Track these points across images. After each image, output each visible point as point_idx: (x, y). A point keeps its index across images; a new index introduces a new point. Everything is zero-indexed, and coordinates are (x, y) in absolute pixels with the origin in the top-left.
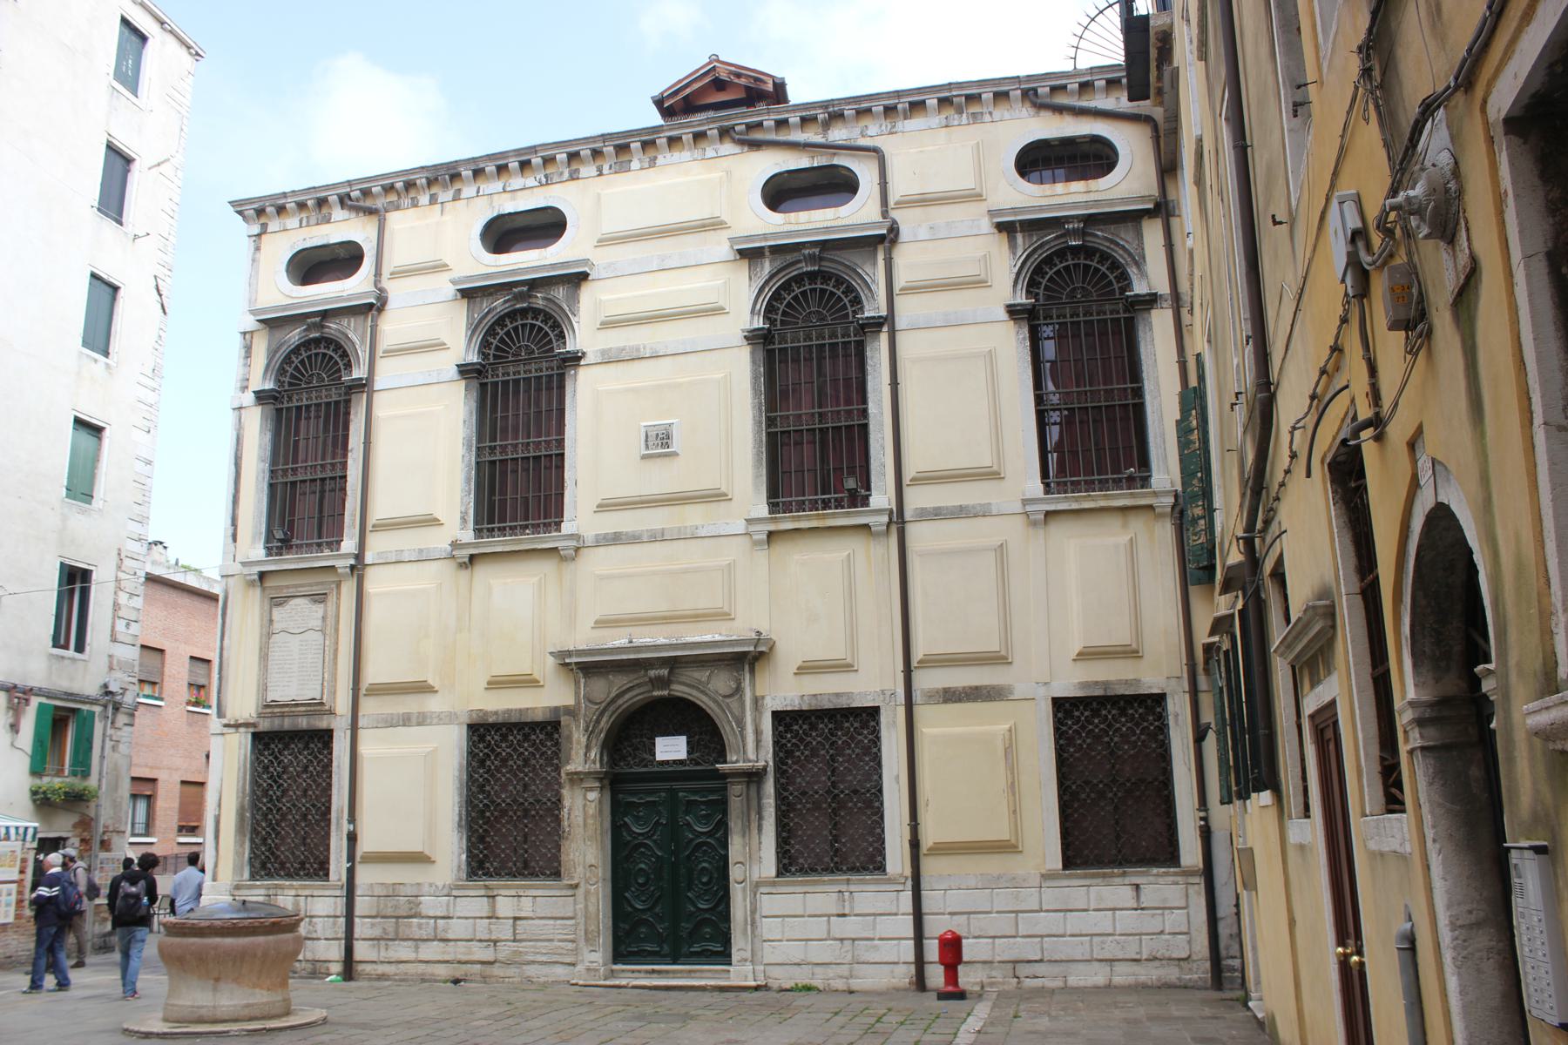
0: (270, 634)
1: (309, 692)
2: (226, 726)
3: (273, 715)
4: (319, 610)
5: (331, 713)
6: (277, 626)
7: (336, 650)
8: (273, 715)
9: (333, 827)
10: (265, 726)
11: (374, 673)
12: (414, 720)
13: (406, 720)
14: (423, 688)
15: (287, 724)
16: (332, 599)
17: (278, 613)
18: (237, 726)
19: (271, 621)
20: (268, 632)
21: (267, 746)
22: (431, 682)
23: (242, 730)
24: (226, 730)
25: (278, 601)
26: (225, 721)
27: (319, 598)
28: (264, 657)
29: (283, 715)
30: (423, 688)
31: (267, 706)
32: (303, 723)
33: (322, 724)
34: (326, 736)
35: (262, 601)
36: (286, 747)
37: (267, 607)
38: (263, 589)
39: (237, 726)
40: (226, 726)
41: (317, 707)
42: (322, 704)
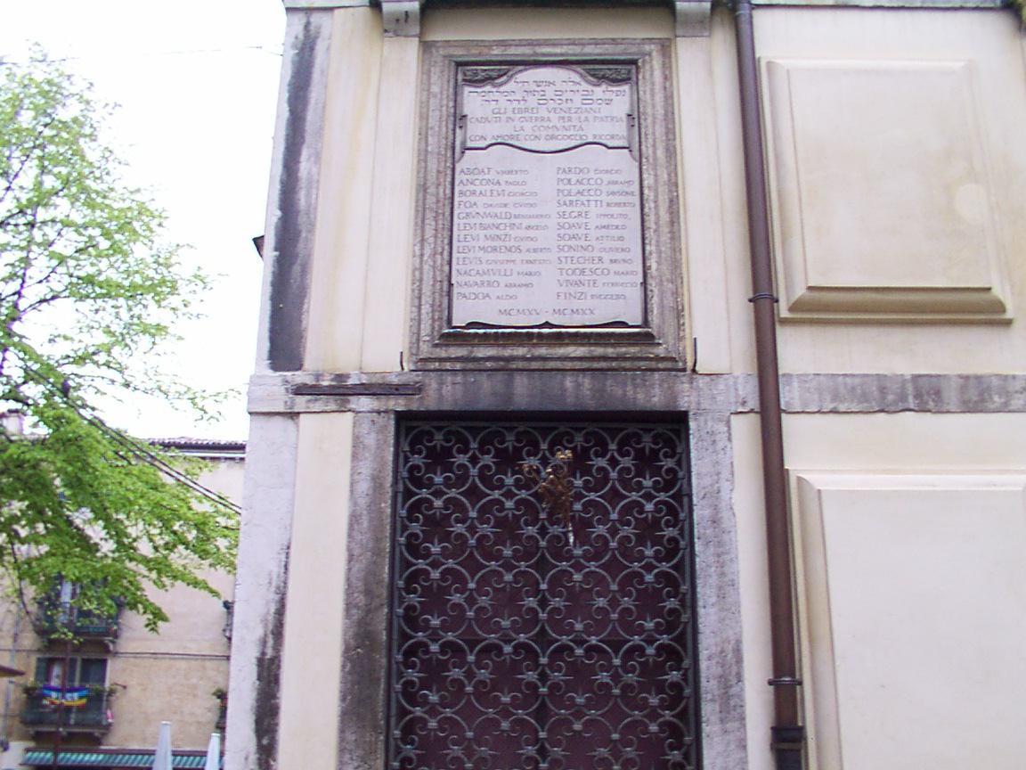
0: (455, 151)
1: (611, 300)
2: (300, 390)
3: (472, 366)
4: (617, 100)
5: (675, 366)
6: (476, 131)
7: (673, 203)
8: (472, 366)
9: (709, 710)
10: (443, 393)
11: (816, 256)
12: (951, 395)
13: (925, 395)
14: (976, 311)
15: (524, 393)
16: (653, 70)
17: (475, 101)
18: (340, 391)
19: (459, 119)
20: (446, 148)
21: (440, 459)
22: (1000, 292)
23: (365, 403)
24: (301, 403)
25: (480, 71)
26: (300, 377)
27: (613, 70)
28: (437, 208)
29: (505, 368)
30: (976, 311)
31: (455, 337)
32: (577, 391)
33: (652, 395)
34: (672, 426)
35: (425, 73)
36: (508, 460)
37: (440, 83)
38: (426, 47)
39: (340, 391)
40: (300, 390)
41: (634, 345)
42: (647, 338)
